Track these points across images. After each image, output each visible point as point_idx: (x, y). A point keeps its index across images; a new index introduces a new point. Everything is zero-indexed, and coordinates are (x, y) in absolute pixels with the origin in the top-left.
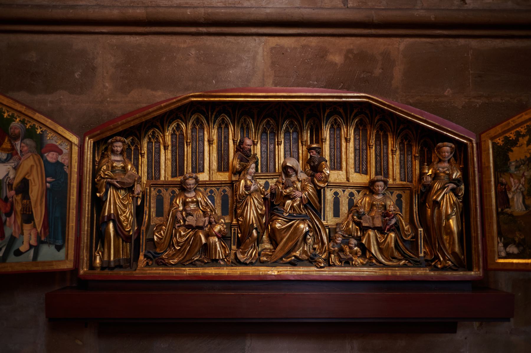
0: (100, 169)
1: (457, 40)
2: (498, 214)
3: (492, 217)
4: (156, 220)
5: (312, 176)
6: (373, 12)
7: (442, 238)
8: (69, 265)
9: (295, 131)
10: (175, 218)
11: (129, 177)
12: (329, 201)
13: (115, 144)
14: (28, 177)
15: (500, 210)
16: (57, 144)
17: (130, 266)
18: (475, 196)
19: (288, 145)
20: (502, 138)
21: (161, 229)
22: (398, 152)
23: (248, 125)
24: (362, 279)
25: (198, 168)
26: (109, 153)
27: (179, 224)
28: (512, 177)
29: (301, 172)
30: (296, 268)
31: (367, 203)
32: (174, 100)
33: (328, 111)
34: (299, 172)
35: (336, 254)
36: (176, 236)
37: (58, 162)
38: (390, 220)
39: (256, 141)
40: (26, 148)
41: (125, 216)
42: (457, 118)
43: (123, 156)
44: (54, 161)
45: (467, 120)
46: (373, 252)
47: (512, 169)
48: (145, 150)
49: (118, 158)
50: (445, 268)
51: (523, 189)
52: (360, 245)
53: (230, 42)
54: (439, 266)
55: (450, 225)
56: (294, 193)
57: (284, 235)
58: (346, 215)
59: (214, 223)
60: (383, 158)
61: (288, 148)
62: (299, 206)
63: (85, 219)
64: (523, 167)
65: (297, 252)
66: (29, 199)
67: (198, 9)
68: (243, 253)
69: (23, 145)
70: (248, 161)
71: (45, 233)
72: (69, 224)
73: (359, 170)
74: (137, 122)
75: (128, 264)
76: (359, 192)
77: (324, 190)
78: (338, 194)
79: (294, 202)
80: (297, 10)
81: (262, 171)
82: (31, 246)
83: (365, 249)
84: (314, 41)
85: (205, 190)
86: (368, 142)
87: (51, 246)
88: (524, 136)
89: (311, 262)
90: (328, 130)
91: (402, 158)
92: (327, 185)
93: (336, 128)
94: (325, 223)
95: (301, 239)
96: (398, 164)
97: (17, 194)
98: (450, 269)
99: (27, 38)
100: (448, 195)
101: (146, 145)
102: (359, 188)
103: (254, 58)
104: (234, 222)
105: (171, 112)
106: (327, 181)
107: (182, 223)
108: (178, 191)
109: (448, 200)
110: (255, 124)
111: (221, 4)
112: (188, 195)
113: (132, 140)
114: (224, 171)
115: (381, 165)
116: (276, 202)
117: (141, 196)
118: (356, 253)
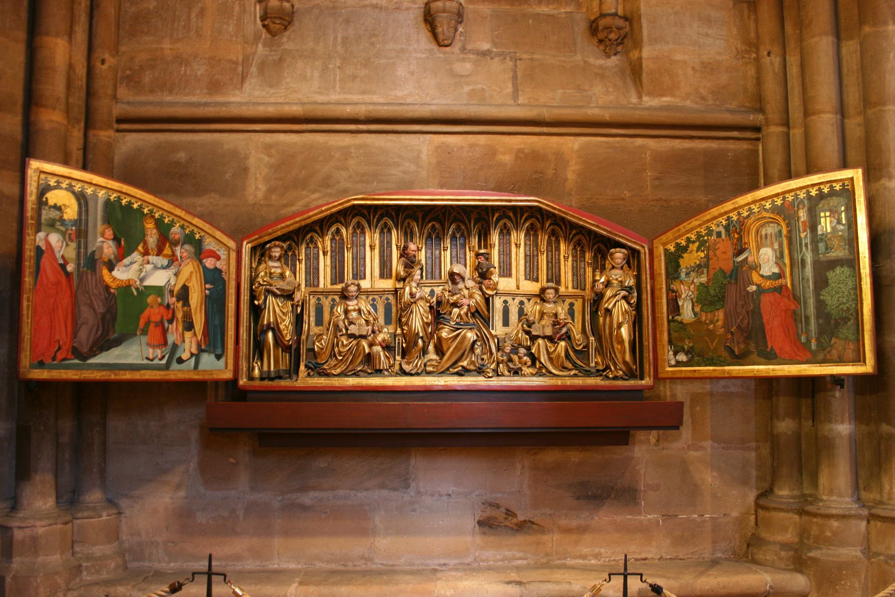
0: (257, 276)
1: (634, 139)
2: (669, 322)
3: (663, 325)
6: (545, 110)
8: (228, 375)
9: (462, 235)
10: (337, 327)
11: (288, 283)
12: (497, 310)
13: (273, 250)
14: (188, 283)
15: (670, 317)
16: (215, 249)
18: (647, 304)
20: (673, 244)
22: (570, 259)
23: (411, 230)
25: (359, 274)
26: (267, 259)
27: (341, 333)
28: (683, 284)
29: (469, 279)
30: (463, 378)
31: (537, 312)
32: (336, 204)
33: (497, 215)
34: (466, 279)
36: (338, 345)
37: (216, 268)
38: (561, 329)
39: (420, 246)
40: (185, 254)
41: (285, 325)
43: (281, 262)
46: (542, 361)
47: (683, 275)
48: (303, 256)
49: (277, 264)
50: (615, 378)
51: (693, 296)
54: (611, 376)
55: (621, 333)
58: (516, 324)
59: (378, 332)
60: (555, 264)
61: (454, 254)
62: (467, 314)
63: (243, 328)
66: (189, 306)
67: (359, 106)
68: (408, 363)
72: (227, 332)
73: (530, 277)
74: (297, 226)
75: (288, 376)
76: (529, 300)
77: (493, 298)
78: (508, 302)
79: (461, 310)
80: (463, 108)
82: (192, 355)
83: (534, 359)
84: (482, 139)
85: (367, 298)
86: (539, 248)
87: (211, 354)
88: (694, 242)
91: (575, 265)
92: (496, 293)
93: (505, 232)
94: (493, 332)
95: (468, 348)
97: (178, 301)
98: (622, 378)
102: (530, 297)
104: (399, 331)
105: (332, 215)
106: (496, 289)
107: (344, 331)
108: (338, 299)
112: (349, 303)
113: (290, 245)
115: (552, 273)
116: (442, 311)
117: (300, 303)
118: (526, 363)
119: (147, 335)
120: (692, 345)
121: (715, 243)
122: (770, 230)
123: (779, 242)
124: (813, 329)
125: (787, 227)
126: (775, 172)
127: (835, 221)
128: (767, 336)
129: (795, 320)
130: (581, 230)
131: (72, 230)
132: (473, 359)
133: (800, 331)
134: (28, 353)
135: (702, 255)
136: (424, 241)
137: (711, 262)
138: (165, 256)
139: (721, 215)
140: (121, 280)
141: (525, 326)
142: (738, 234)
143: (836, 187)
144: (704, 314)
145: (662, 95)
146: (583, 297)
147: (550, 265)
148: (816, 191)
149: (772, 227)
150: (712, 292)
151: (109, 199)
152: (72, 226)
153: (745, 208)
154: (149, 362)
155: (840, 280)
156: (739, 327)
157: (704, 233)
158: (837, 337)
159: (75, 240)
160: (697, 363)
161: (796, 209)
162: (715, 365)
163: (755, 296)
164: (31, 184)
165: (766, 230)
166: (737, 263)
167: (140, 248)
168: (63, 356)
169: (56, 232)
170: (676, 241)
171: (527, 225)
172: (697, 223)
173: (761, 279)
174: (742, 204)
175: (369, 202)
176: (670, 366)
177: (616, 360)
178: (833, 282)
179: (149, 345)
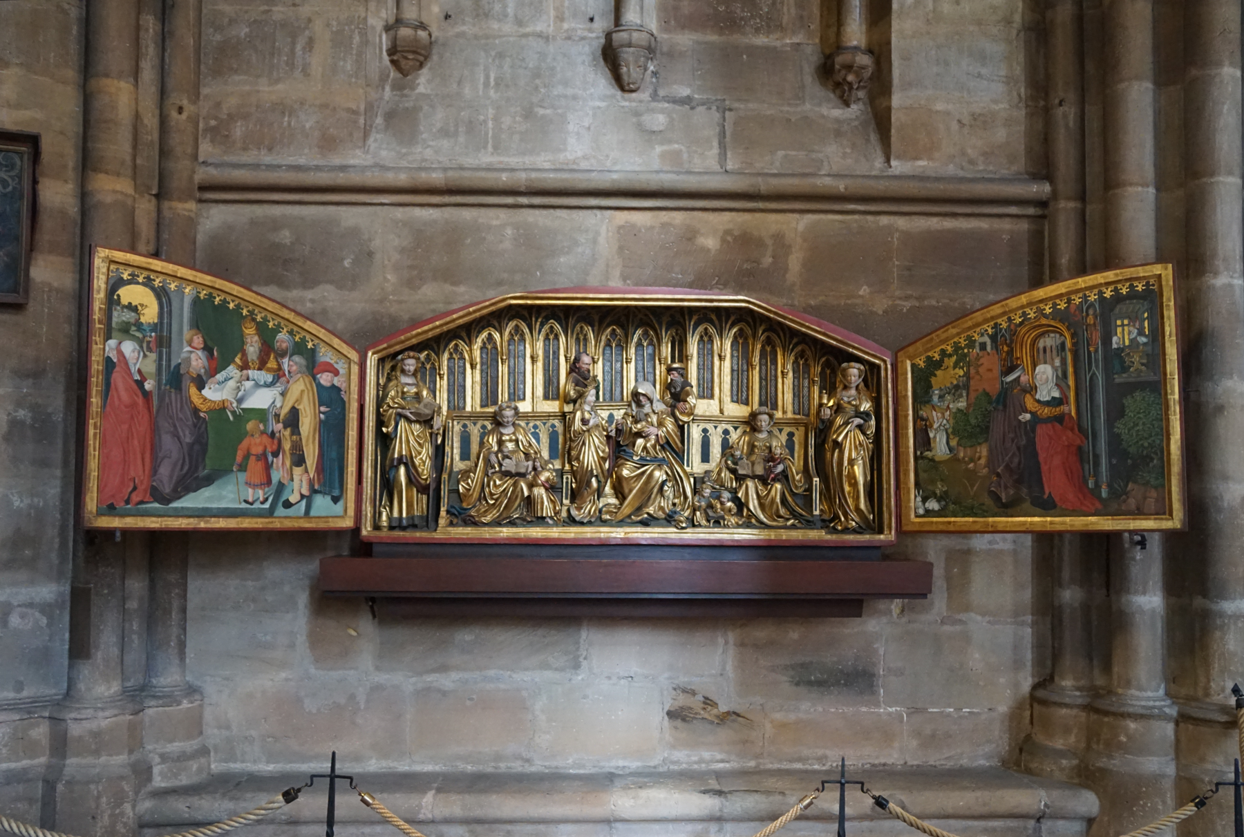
1: (878, 218)
2: (916, 458)
3: (908, 462)
4: (459, 465)
5: (673, 407)
6: (760, 179)
8: (348, 523)
9: (651, 343)
11: (426, 406)
15: (919, 453)
16: (332, 362)
17: (427, 526)
19: (640, 363)
20: (923, 358)
21: (469, 477)
22: (791, 375)
23: (586, 335)
24: (736, 544)
25: (516, 394)
26: (398, 373)
27: (493, 470)
29: (658, 401)
30: (649, 529)
32: (487, 303)
34: (654, 401)
35: (703, 511)
36: (489, 486)
37: (333, 386)
38: (775, 466)
40: (294, 368)
41: (421, 459)
43: (416, 377)
44: (328, 384)
46: (751, 508)
47: (935, 399)
48: (445, 370)
50: (846, 530)
51: (947, 426)
52: (736, 500)
53: (560, 217)
54: (840, 528)
55: (854, 472)
56: (647, 430)
57: (633, 485)
58: (718, 460)
59: (540, 469)
62: (654, 447)
65: (651, 508)
68: (579, 509)
69: (291, 363)
70: (586, 386)
71: (319, 479)
73: (738, 399)
76: (736, 428)
77: (689, 426)
79: (647, 442)
81: (604, 400)
82: (302, 496)
83: (741, 505)
84: (678, 217)
85: (527, 424)
87: (326, 496)
88: (950, 356)
89: (669, 522)
90: (696, 343)
91: (796, 383)
92: (693, 419)
93: (706, 340)
94: (688, 469)
95: (655, 490)
96: (791, 391)
98: (855, 531)
99: (277, 211)
101: (446, 363)
102: (736, 424)
103: (595, 241)
104: (567, 467)
105: (482, 318)
106: (692, 414)
107: (497, 469)
110: (596, 333)
111: (549, 163)
112: (504, 431)
113: (428, 355)
114: (553, 399)
117: (441, 432)
118: (730, 510)
119: (245, 471)
121: (978, 358)
122: (1049, 341)
123: (1062, 358)
125: (1072, 338)
126: (1065, 259)
127: (1136, 331)
128: (1044, 479)
130: (805, 339)
131: (151, 337)
132: (662, 504)
134: (95, 495)
135: (961, 373)
136: (601, 350)
137: (972, 383)
138: (269, 370)
139: (986, 321)
140: (215, 402)
141: (729, 462)
142: (1008, 346)
143: (1137, 286)
145: (916, 158)
146: (806, 426)
147: (764, 383)
148: (1111, 291)
150: (973, 421)
151: (198, 297)
152: (152, 331)
154: (248, 506)
155: (1141, 409)
156: (1007, 467)
158: (1135, 482)
159: (154, 350)
161: (1084, 314)
162: (975, 515)
164: (98, 277)
166: (1006, 383)
167: (237, 360)
168: (138, 499)
169: (130, 340)
171: (735, 330)
172: (954, 331)
173: (1036, 405)
174: (1014, 307)
175: (529, 302)
178: (1131, 411)
179: (248, 484)
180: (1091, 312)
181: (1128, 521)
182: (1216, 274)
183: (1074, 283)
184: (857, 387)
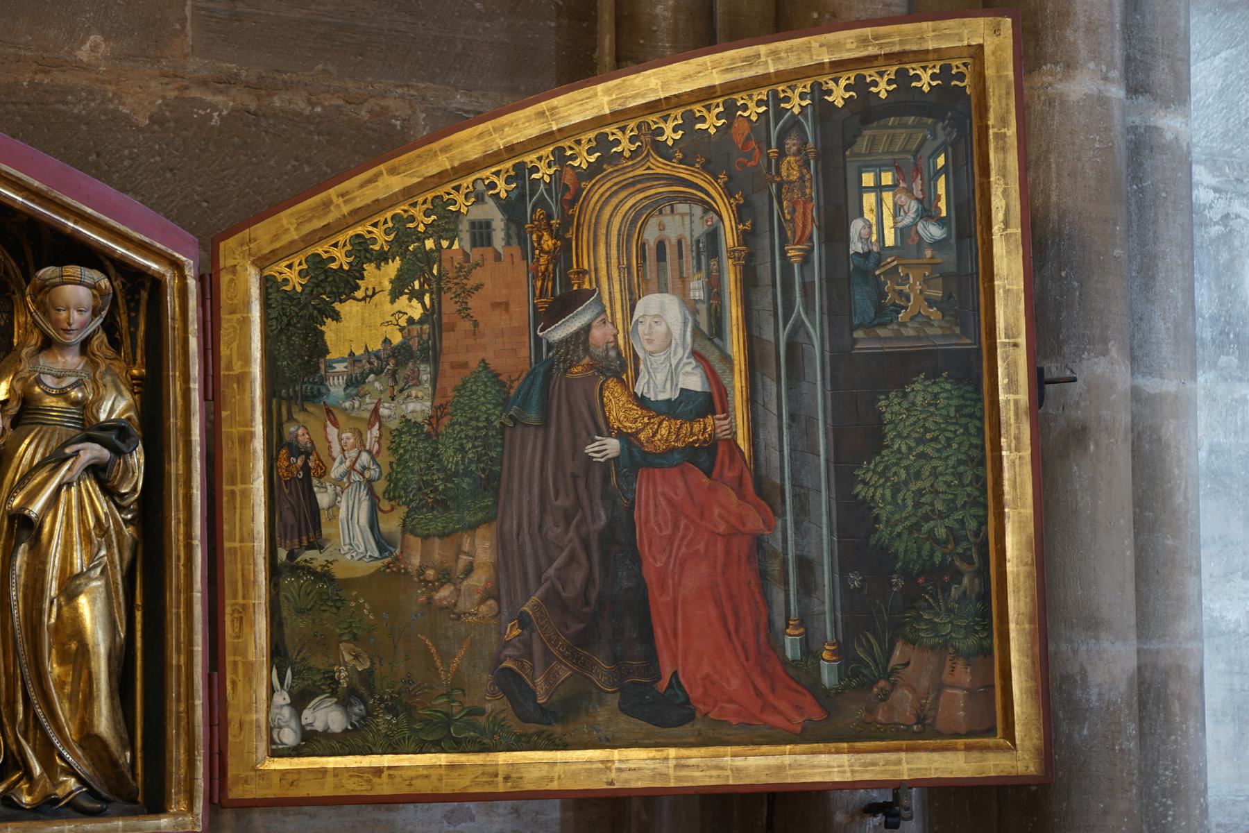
2: (274, 570)
3: (249, 584)
7: (40, 676)
15: (282, 554)
18: (188, 498)
28: (335, 424)
42: (126, 163)
45: (168, 175)
47: (336, 388)
51: (373, 473)
54: (26, 799)
55: (76, 618)
64: (377, 384)
88: (382, 258)
100: (73, 490)
109: (74, 513)
120: (368, 665)
121: (467, 266)
123: (709, 275)
124: (827, 608)
125: (740, 219)
127: (914, 206)
128: (659, 634)
129: (763, 575)
133: (779, 622)
135: (416, 311)
137: (448, 340)
139: (493, 158)
142: (555, 235)
144: (415, 542)
148: (847, 88)
149: (682, 215)
153: (584, 138)
155: (927, 430)
157: (422, 221)
160: (386, 735)
161: (773, 150)
162: (458, 746)
163: (614, 480)
165: (662, 227)
166: (550, 346)
170: (310, 251)
173: (637, 412)
174: (576, 119)
176: (275, 754)
177: (50, 731)
178: (899, 435)
180: (791, 144)
181: (893, 756)
182: (1070, 66)
183: (747, 59)
184: (85, 346)
